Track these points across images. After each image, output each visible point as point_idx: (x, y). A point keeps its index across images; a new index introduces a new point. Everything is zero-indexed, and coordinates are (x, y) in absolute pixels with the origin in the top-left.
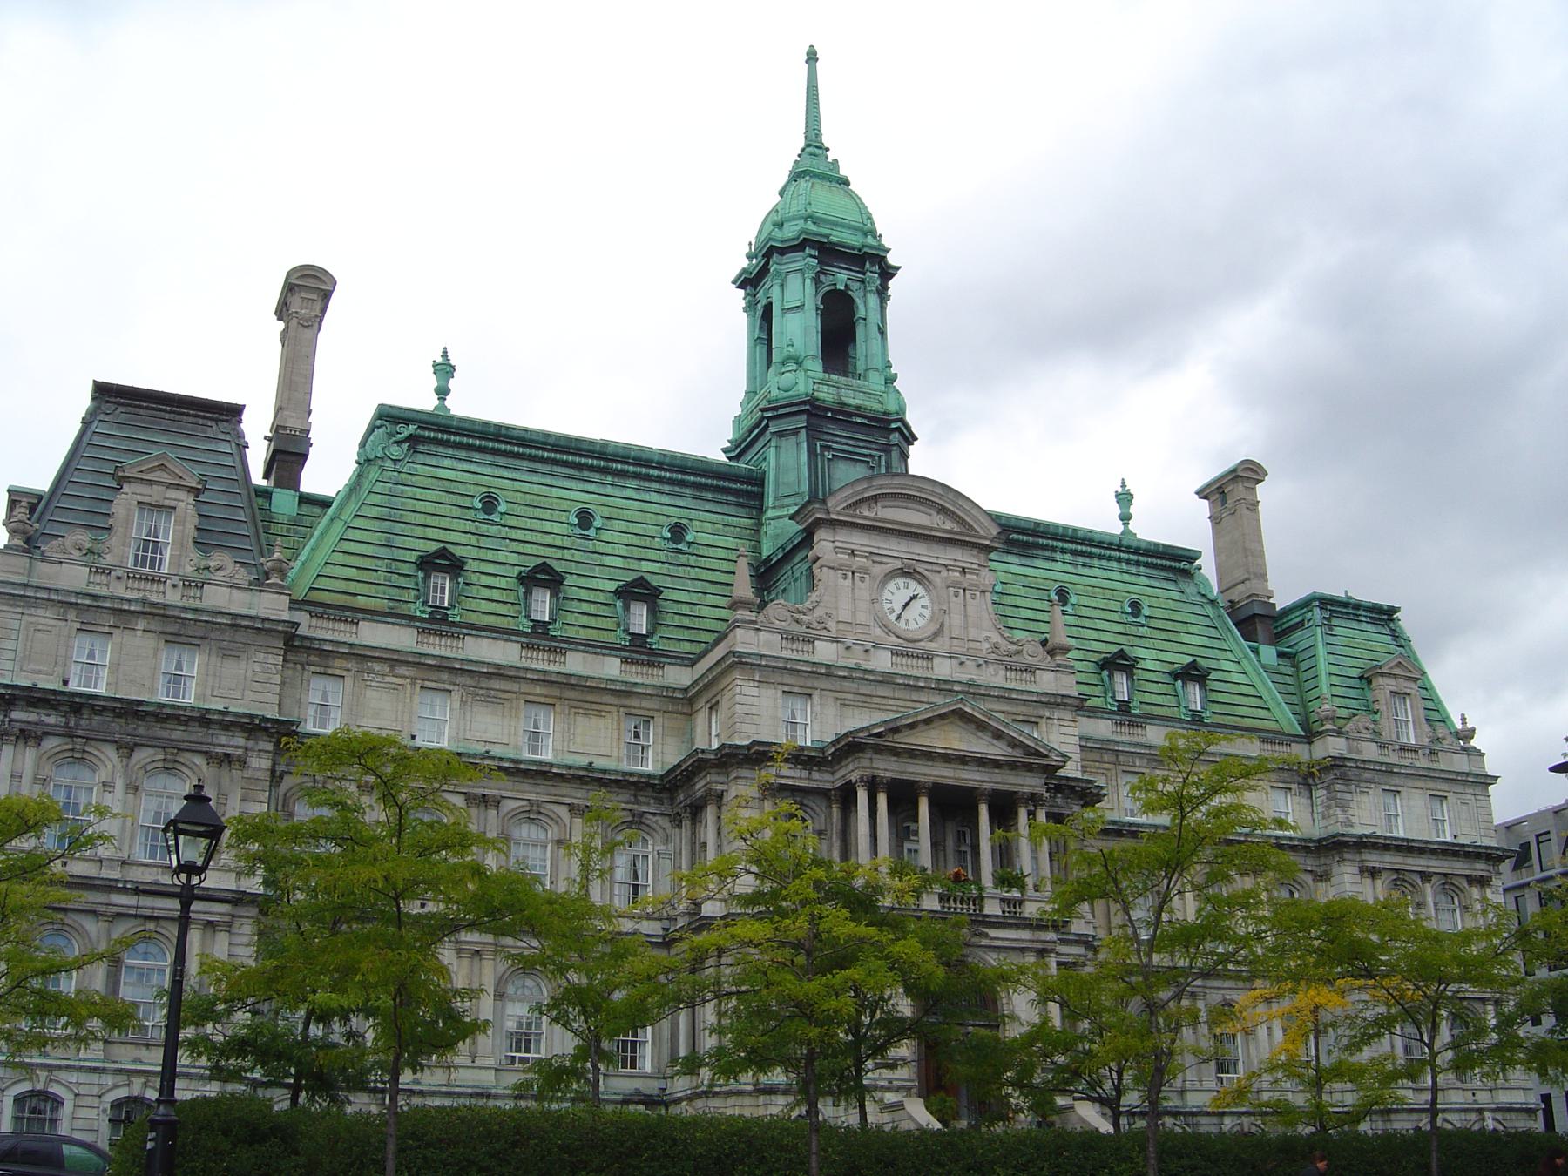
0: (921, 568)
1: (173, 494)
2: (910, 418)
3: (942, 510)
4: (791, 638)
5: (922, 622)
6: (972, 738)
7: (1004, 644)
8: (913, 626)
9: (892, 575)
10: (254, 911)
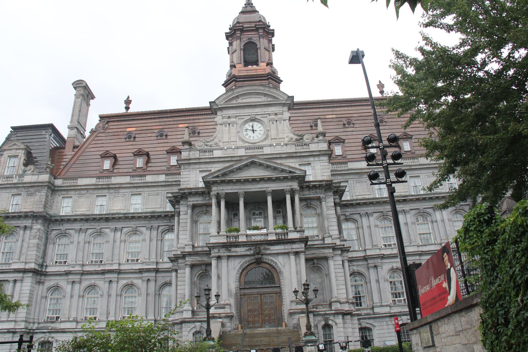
0: (257, 117)
1: (18, 151)
2: (280, 75)
3: (265, 95)
4: (205, 151)
5: (259, 136)
6: (262, 171)
7: (295, 137)
8: (256, 138)
9: (246, 122)
10: (30, 275)
